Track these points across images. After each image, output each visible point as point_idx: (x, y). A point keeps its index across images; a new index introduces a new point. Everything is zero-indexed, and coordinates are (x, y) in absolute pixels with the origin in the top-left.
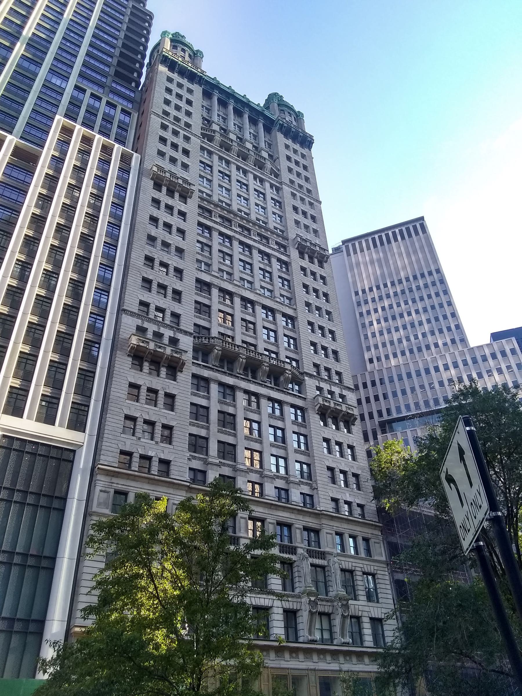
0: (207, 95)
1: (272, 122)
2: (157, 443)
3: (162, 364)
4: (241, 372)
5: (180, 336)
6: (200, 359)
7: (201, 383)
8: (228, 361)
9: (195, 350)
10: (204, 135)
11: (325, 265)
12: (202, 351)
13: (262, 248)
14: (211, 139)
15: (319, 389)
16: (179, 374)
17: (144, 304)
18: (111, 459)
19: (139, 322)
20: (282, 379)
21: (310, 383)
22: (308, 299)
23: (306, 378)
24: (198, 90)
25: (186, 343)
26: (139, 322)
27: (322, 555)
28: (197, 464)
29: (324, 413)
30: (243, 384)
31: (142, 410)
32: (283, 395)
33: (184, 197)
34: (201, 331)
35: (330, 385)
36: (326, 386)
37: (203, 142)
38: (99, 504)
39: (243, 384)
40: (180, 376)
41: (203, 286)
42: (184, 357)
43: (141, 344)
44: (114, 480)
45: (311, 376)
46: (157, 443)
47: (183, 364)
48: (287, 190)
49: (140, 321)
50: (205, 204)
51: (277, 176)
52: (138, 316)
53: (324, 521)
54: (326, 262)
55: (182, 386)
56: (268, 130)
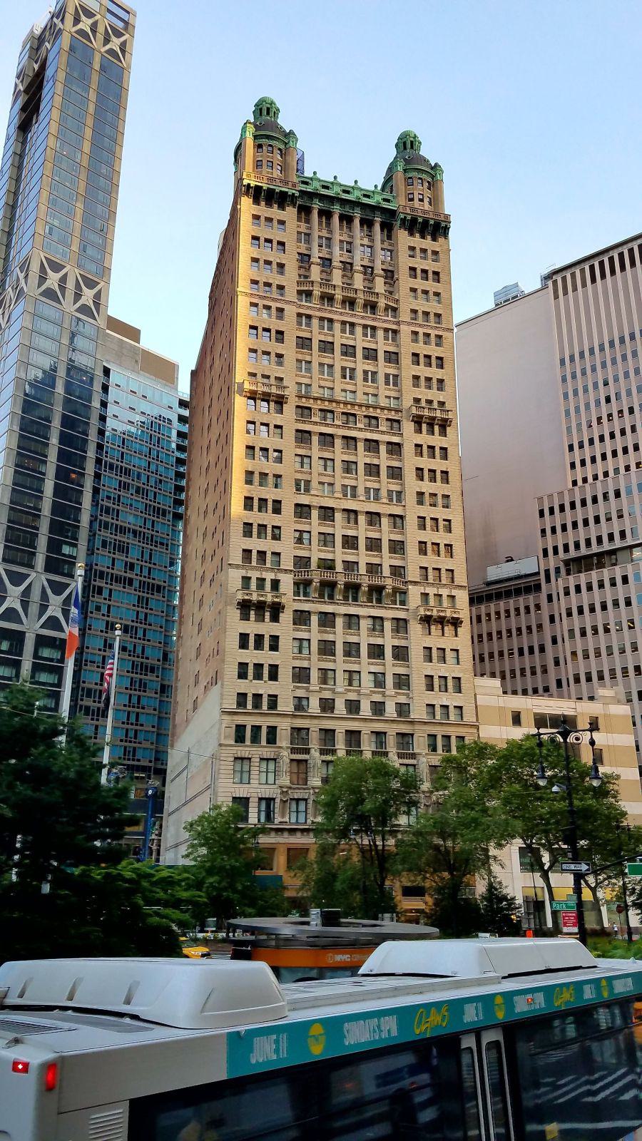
0: (304, 211)
1: (392, 213)
2: (265, 682)
3: (266, 609)
4: (341, 598)
5: (281, 576)
6: (302, 594)
7: (301, 618)
8: (328, 588)
9: (296, 584)
10: (300, 293)
11: (448, 429)
12: (302, 586)
13: (370, 436)
14: (309, 294)
15: (425, 595)
16: (281, 615)
17: (247, 552)
18: (231, 701)
19: (243, 573)
20: (384, 593)
21: (414, 593)
22: (420, 487)
23: (410, 587)
24: (290, 213)
25: (287, 582)
26: (243, 573)
27: (413, 756)
28: (301, 693)
29: (427, 620)
30: (343, 610)
31: (251, 656)
32: (384, 611)
33: (280, 401)
34: (301, 562)
35: (438, 588)
36: (431, 591)
37: (300, 306)
38: (225, 737)
39: (343, 610)
40: (282, 616)
41: (302, 511)
42: (283, 600)
43: (246, 597)
44: (235, 717)
45: (415, 583)
46: (265, 682)
47: (284, 607)
48: (405, 330)
49: (244, 571)
50: (304, 402)
51: (395, 310)
52: (243, 567)
53: (417, 727)
54: (450, 426)
55: (284, 628)
56: (387, 228)
